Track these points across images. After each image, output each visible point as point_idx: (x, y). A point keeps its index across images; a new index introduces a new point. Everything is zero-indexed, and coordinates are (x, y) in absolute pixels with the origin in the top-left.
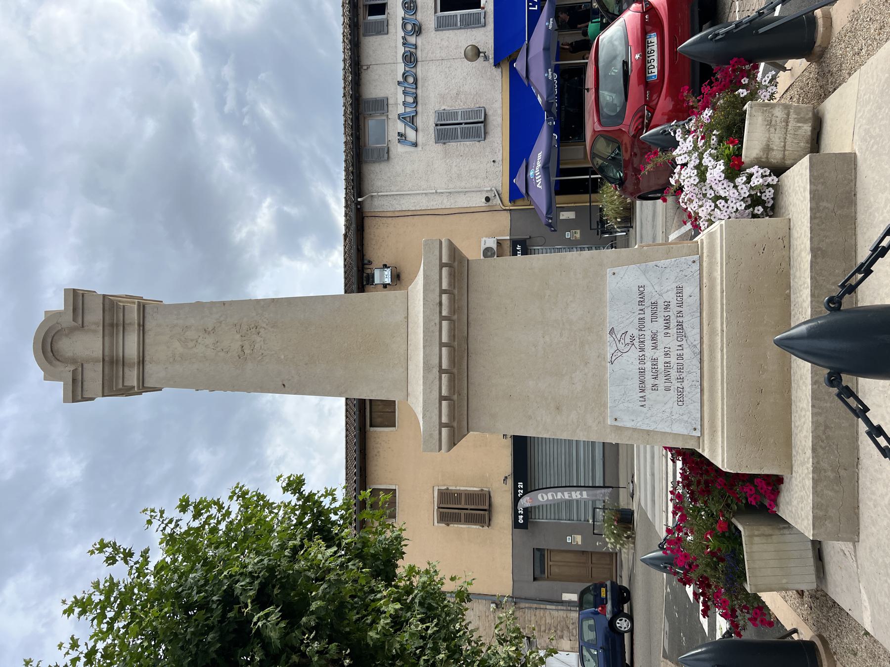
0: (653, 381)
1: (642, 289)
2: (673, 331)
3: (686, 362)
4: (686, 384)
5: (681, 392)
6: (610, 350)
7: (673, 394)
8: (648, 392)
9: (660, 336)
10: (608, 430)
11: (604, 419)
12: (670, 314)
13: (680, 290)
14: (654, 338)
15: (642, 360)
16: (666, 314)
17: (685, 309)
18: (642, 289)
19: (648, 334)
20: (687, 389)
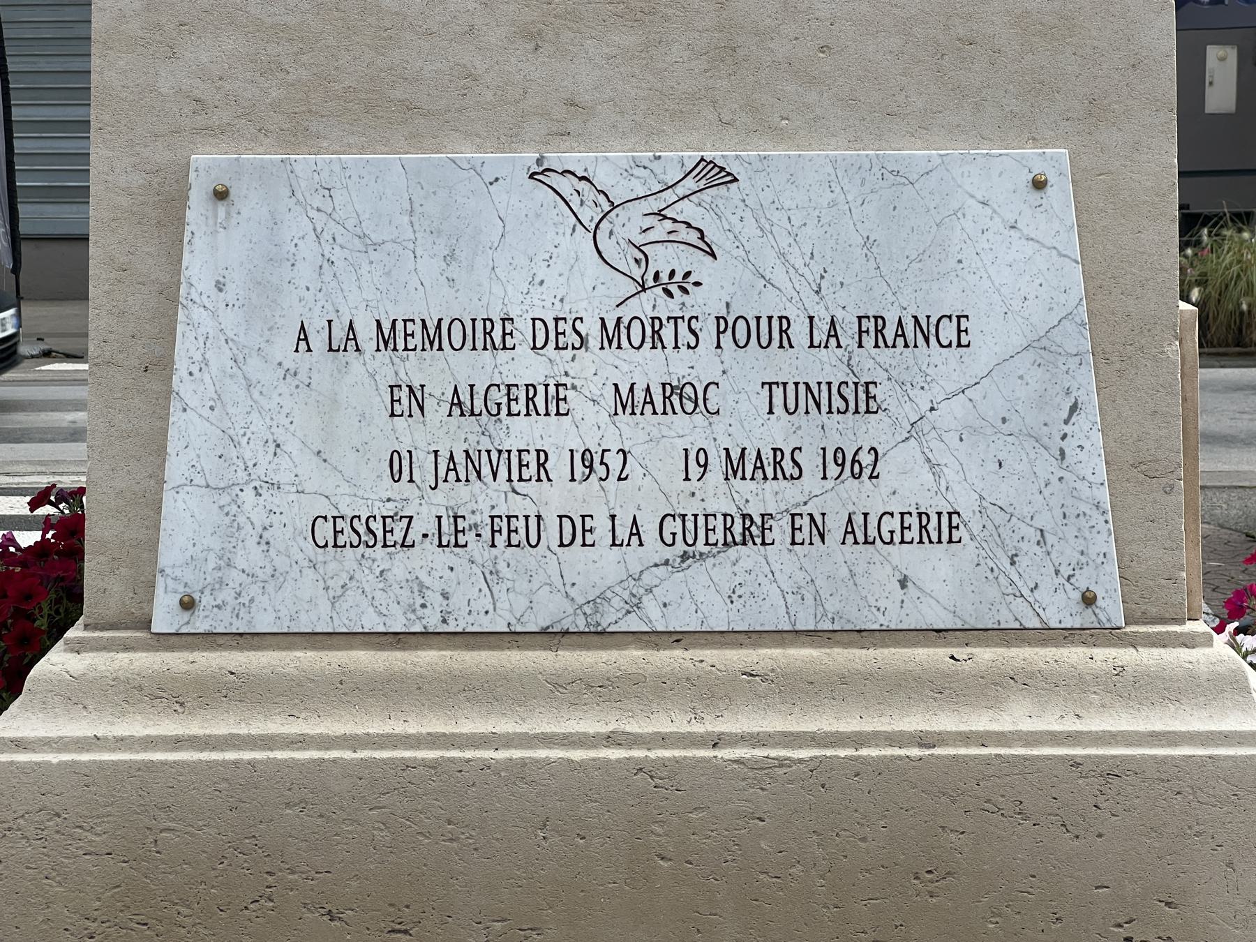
0: (438, 389)
1: (948, 332)
2: (717, 496)
3: (546, 561)
4: (428, 560)
5: (379, 533)
6: (609, 165)
7: (372, 495)
8: (385, 367)
9: (686, 430)
10: (160, 155)
11: (216, 133)
12: (812, 479)
13: (935, 528)
14: (677, 396)
15: (556, 333)
16: (809, 460)
17: (836, 554)
18: (948, 332)
19: (696, 365)
20: (401, 565)
